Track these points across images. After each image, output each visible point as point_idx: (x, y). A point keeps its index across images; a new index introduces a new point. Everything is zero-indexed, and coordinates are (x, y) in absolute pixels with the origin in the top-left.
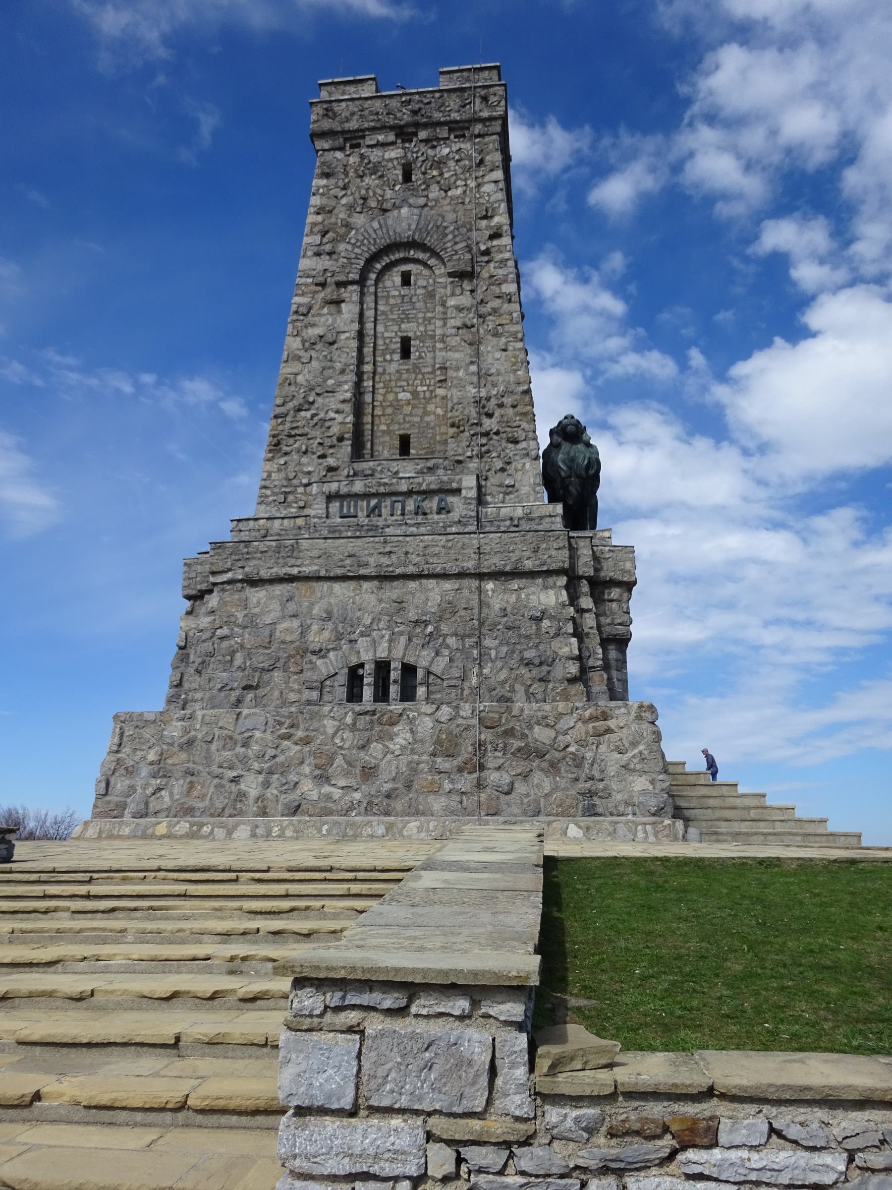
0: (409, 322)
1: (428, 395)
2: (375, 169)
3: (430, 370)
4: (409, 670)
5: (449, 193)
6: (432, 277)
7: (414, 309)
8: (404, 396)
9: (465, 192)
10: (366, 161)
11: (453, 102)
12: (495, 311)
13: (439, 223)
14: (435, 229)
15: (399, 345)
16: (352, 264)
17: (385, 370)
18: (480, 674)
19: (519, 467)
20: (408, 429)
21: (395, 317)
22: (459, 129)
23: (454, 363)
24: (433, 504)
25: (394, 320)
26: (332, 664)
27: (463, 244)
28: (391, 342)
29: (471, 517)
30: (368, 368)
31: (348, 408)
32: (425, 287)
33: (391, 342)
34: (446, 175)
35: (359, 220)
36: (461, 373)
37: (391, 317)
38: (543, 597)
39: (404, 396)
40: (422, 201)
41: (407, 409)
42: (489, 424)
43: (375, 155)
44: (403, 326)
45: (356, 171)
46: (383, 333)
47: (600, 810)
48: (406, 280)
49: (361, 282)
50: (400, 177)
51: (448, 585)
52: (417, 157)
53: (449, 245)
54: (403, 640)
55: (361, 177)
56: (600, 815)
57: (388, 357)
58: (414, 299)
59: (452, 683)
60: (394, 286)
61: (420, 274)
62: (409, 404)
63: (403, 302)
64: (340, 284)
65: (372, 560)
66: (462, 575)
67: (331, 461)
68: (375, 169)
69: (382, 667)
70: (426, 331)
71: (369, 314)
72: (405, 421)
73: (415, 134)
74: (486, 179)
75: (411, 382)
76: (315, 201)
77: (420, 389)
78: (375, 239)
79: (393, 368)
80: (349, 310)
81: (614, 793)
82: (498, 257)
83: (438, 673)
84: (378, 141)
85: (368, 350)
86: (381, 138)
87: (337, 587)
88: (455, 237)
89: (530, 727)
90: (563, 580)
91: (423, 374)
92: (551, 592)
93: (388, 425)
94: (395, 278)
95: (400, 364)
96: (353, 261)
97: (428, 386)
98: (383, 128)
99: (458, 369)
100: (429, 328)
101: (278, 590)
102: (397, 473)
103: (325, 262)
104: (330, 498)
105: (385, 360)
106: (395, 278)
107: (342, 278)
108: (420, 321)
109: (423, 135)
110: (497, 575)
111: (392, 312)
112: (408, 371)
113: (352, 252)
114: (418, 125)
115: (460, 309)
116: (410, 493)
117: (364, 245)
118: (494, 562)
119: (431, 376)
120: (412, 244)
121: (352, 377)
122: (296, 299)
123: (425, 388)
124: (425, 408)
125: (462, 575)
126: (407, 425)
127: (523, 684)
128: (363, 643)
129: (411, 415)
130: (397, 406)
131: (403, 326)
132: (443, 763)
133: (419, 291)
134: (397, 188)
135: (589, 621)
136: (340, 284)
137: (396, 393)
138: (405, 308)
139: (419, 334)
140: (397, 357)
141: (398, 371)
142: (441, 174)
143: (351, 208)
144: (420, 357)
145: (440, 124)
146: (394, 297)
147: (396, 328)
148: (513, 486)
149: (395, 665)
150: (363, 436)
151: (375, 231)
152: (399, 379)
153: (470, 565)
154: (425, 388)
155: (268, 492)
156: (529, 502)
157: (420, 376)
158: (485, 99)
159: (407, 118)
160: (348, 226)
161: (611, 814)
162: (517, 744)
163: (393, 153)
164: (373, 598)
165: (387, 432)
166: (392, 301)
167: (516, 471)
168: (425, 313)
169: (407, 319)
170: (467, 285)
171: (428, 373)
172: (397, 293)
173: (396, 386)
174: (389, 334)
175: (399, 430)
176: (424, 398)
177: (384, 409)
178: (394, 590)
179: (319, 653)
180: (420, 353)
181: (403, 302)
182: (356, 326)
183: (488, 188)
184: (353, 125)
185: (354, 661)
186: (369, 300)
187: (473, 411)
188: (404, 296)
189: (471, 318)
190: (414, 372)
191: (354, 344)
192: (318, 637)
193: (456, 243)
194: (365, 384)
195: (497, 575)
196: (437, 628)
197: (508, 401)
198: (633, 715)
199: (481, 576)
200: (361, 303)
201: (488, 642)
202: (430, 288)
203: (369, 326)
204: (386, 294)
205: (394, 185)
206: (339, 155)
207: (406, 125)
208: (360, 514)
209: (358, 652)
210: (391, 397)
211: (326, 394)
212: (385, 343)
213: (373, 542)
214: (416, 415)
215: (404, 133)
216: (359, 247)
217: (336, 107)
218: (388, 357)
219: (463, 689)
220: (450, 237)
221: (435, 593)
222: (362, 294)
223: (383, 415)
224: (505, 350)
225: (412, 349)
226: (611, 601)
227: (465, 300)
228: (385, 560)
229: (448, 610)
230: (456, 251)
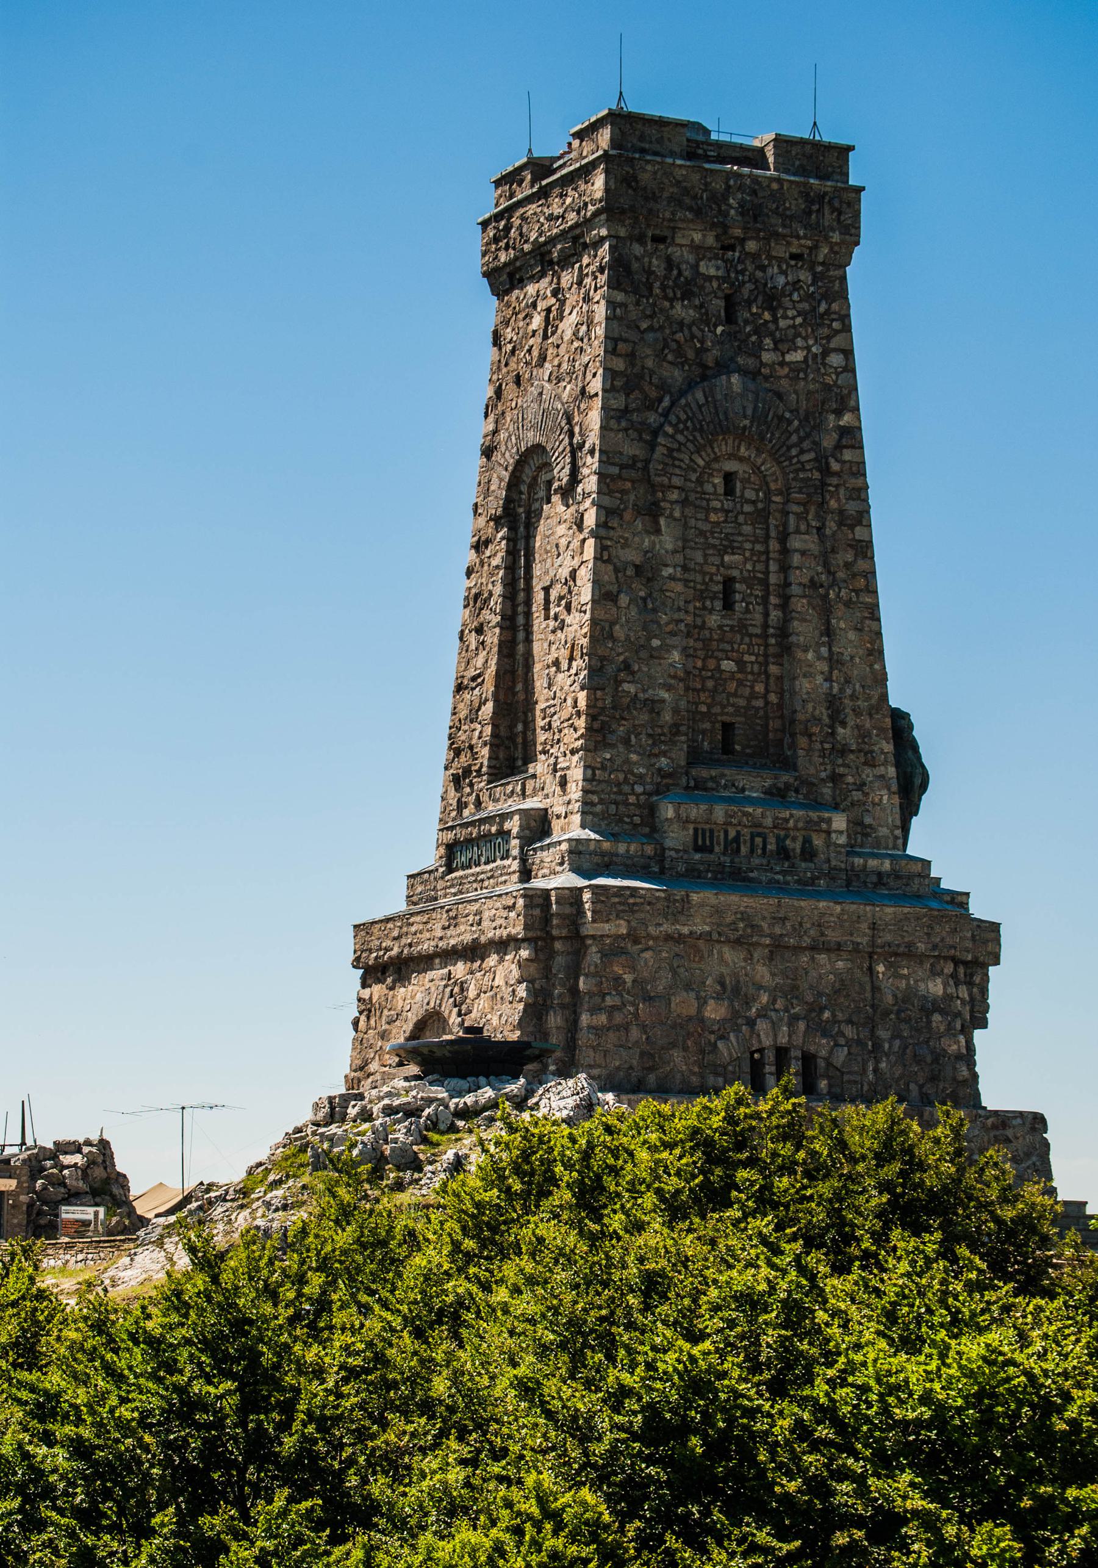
0: (733, 554)
1: (756, 668)
3: (758, 631)
5: (788, 358)
7: (740, 534)
8: (728, 665)
9: (806, 357)
10: (675, 272)
13: (780, 412)
14: (776, 421)
15: (721, 587)
16: (674, 459)
17: (704, 622)
18: (875, 1070)
20: (731, 715)
21: (717, 542)
23: (802, 639)
25: (714, 546)
27: (812, 455)
28: (711, 580)
29: (841, 870)
32: (754, 502)
33: (711, 580)
34: (782, 323)
36: (810, 655)
37: (711, 541)
38: (931, 985)
39: (728, 665)
40: (751, 362)
41: (732, 686)
44: (726, 558)
45: (663, 288)
46: (701, 565)
50: (723, 313)
52: (744, 283)
53: (794, 452)
54: (802, 1025)
55: (671, 301)
57: (708, 603)
58: (741, 519)
59: (852, 1078)
60: (715, 493)
61: (748, 481)
62: (732, 678)
63: (725, 521)
69: (782, 1053)
70: (754, 571)
72: (729, 704)
75: (736, 646)
77: (746, 658)
78: (700, 422)
83: (839, 1066)
88: (801, 440)
91: (751, 636)
92: (939, 981)
93: (709, 706)
95: (723, 617)
96: (675, 454)
97: (757, 655)
99: (806, 651)
100: (759, 567)
102: (743, 790)
105: (704, 608)
108: (747, 554)
111: (712, 533)
112: (732, 627)
117: (687, 428)
119: (760, 641)
123: (753, 658)
124: (752, 687)
126: (730, 709)
127: (916, 1083)
128: (762, 1025)
129: (735, 695)
131: (726, 558)
133: (748, 508)
134: (719, 329)
137: (719, 660)
138: (729, 531)
139: (745, 574)
140: (718, 605)
141: (720, 627)
142: (775, 320)
144: (747, 611)
146: (715, 510)
147: (716, 560)
149: (796, 1053)
151: (700, 407)
152: (721, 640)
154: (753, 658)
155: (595, 799)
156: (887, 848)
157: (747, 640)
166: (713, 517)
167: (874, 804)
168: (753, 543)
171: (756, 635)
172: (719, 506)
175: (722, 714)
176: (752, 673)
177: (703, 680)
180: (748, 604)
181: (725, 521)
188: (727, 512)
190: (739, 632)
193: (802, 452)
198: (1028, 1125)
202: (760, 506)
204: (704, 503)
205: (715, 326)
208: (717, 849)
209: (759, 1035)
210: (711, 664)
212: (704, 583)
214: (741, 696)
216: (682, 432)
220: (794, 438)
223: (703, 689)
225: (738, 597)
230: (802, 464)
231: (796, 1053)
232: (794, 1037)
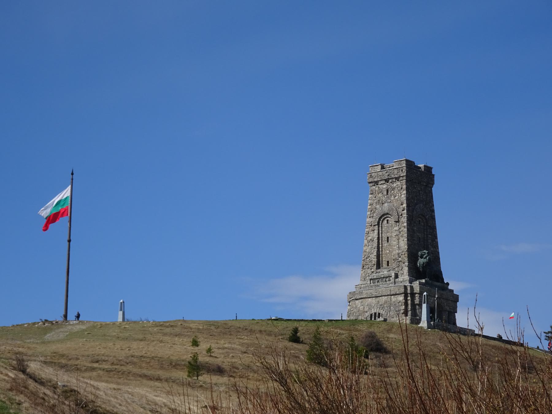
2: (381, 191)
4: (379, 314)
6: (392, 220)
11: (396, 171)
12: (402, 231)
22: (397, 179)
24: (387, 279)
30: (381, 246)
31: (375, 257)
35: (378, 206)
40: (390, 201)
42: (400, 259)
43: (381, 186)
48: (388, 220)
49: (378, 224)
51: (386, 297)
64: (374, 226)
66: (388, 295)
67: (373, 270)
68: (381, 191)
71: (380, 232)
76: (369, 201)
79: (386, 245)
80: (376, 232)
82: (404, 216)
85: (380, 241)
86: (382, 182)
87: (369, 299)
90: (403, 295)
94: (385, 222)
98: (382, 180)
101: (360, 300)
103: (371, 219)
104: (371, 280)
106: (385, 222)
110: (393, 295)
113: (376, 216)
114: (389, 179)
115: (396, 231)
116: (384, 277)
118: (393, 293)
120: (387, 214)
121: (376, 250)
122: (366, 230)
125: (388, 295)
130: (386, 254)
135: (409, 302)
136: (374, 226)
143: (376, 203)
153: (389, 293)
159: (387, 177)
160: (376, 208)
163: (385, 186)
164: (374, 301)
169: (388, 232)
170: (398, 224)
174: (385, 236)
178: (378, 299)
179: (366, 312)
182: (377, 236)
183: (403, 196)
184: (376, 180)
186: (380, 228)
187: (397, 256)
189: (397, 233)
191: (377, 241)
192: (366, 309)
195: (393, 295)
197: (403, 253)
199: (391, 295)
200: (379, 230)
201: (392, 308)
203: (380, 235)
206: (374, 187)
215: (387, 181)
217: (373, 174)
221: (384, 298)
222: (379, 227)
227: (397, 228)
229: (386, 302)
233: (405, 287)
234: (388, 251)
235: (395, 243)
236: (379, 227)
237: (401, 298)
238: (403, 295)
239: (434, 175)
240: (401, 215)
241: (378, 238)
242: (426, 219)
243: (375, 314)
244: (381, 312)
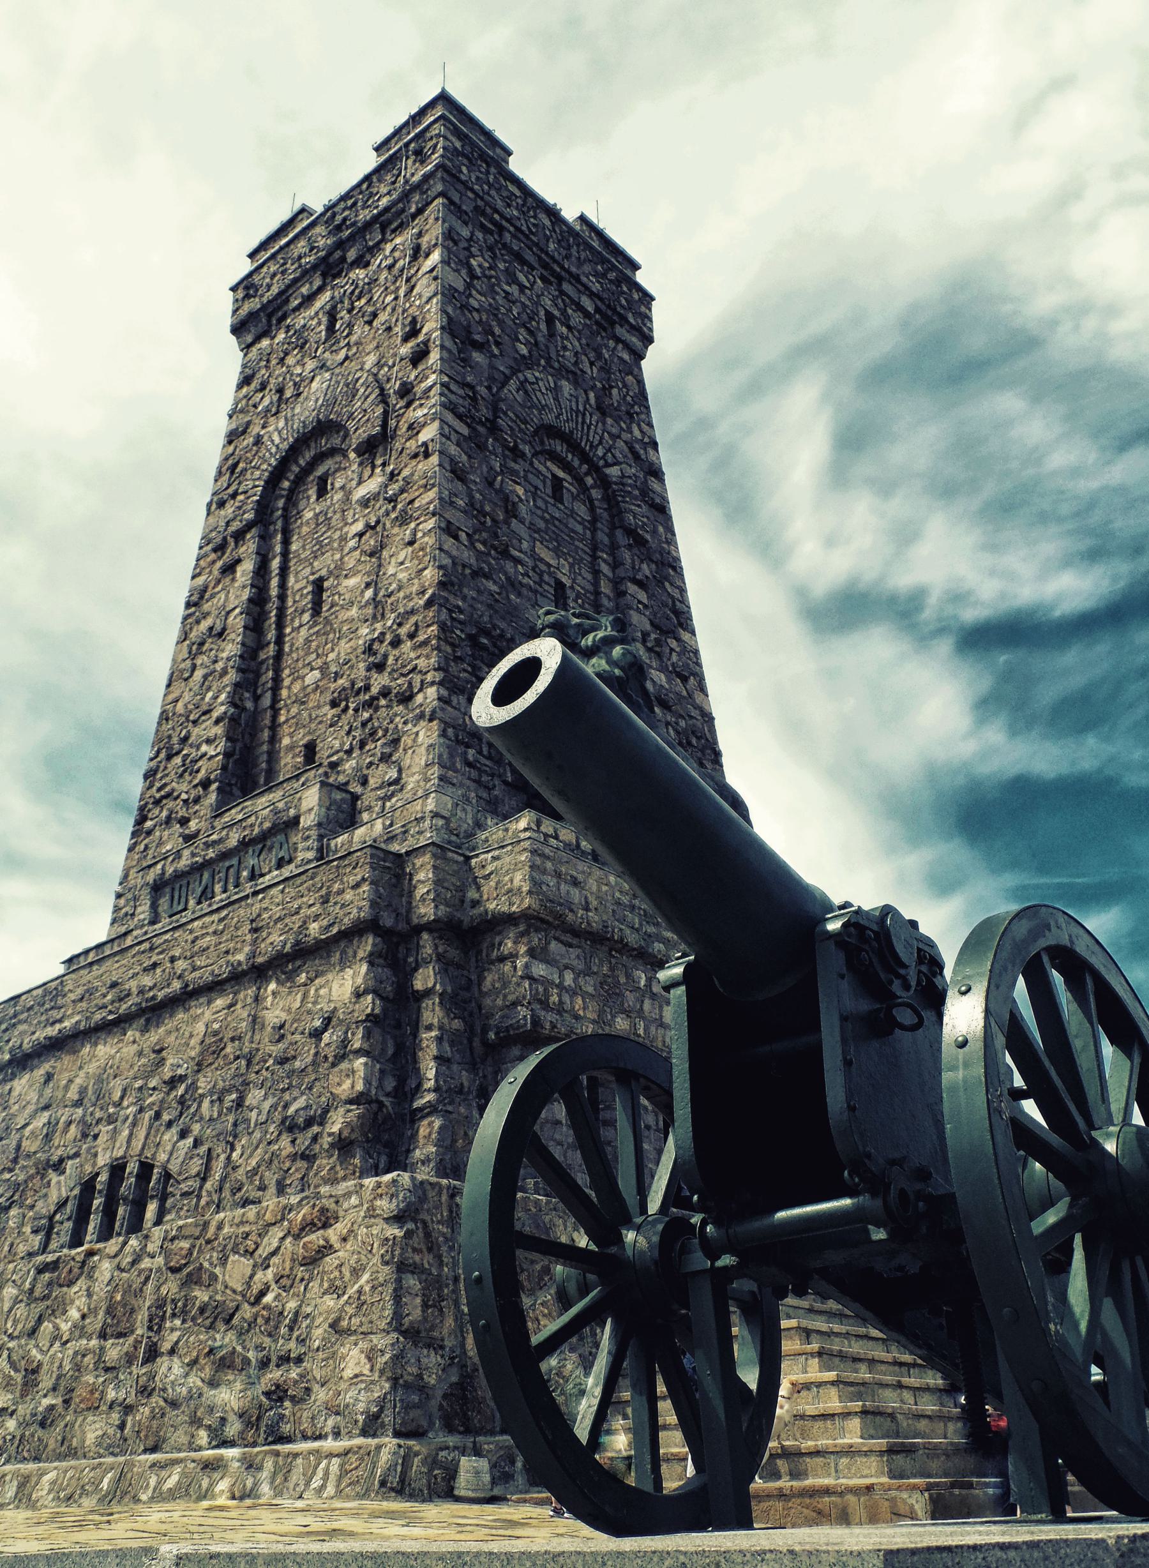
19: (410, 742)
26: (61, 1186)
31: (219, 730)
47: (286, 1428)
56: (288, 1440)
65: (133, 985)
73: (343, 259)
74: (420, 273)
81: (316, 1388)
84: (303, 296)
89: (223, 1261)
90: (368, 944)
107: (236, 525)
109: (352, 255)
114: (341, 245)
125: (237, 977)
132: (114, 1351)
140: (306, 617)
145: (368, 225)
148: (397, 781)
150: (256, 765)
158: (418, 153)
161: (305, 1438)
162: (201, 1295)
165: (291, 748)
173: (304, 666)
185: (88, 1169)
194: (263, 679)
196: (193, 1087)
206: (265, 343)
207: (330, 254)
211: (203, 718)
213: (138, 952)
218: (296, 624)
219: (199, 1197)
222: (265, 538)
224: (411, 543)
226: (502, 959)
228: (147, 981)
231: (132, 1167)
232: (133, 1143)
233: (391, 869)
234: (312, 677)
235: (352, 582)
236: (265, 538)
237: (344, 986)
238: (368, 944)
239: (647, 298)
240: (406, 391)
241: (258, 600)
242: (604, 482)
243: (117, 1170)
244: (172, 1152)
